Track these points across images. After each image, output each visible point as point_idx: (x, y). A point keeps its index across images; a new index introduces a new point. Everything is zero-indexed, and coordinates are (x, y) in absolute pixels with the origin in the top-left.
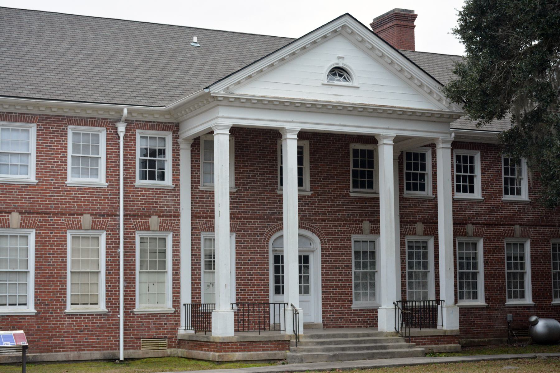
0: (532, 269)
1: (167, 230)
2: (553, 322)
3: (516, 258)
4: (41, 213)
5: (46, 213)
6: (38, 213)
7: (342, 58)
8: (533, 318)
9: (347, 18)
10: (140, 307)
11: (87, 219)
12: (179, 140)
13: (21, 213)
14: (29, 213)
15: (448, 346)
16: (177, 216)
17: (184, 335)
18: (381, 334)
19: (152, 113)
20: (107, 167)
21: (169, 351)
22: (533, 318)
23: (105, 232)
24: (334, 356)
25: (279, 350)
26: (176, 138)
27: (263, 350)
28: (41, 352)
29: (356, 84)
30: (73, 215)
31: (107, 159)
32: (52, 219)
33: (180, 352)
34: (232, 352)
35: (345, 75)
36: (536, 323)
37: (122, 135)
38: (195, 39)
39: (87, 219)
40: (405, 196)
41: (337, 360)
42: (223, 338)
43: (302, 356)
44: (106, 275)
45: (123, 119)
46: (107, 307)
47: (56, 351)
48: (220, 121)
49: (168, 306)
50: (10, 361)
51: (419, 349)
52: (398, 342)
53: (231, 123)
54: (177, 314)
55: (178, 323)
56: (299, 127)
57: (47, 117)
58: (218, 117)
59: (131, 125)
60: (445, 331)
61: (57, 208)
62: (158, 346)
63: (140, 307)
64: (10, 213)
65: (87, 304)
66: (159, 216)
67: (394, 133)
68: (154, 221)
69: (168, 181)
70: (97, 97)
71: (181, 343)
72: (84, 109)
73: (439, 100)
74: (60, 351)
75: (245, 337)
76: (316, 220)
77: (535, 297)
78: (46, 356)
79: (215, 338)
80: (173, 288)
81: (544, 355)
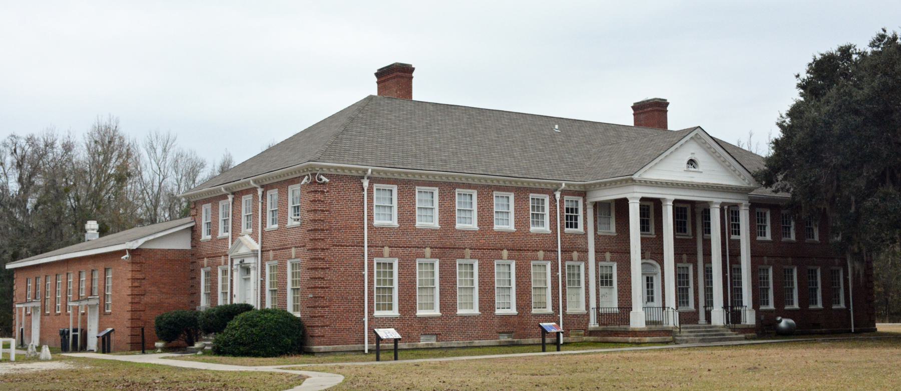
0: (774, 285)
1: (582, 260)
2: (791, 321)
3: (764, 278)
4: (519, 250)
5: (521, 250)
6: (516, 250)
7: (694, 154)
8: (779, 318)
9: (699, 129)
10: (569, 311)
11: (541, 254)
12: (586, 203)
13: (508, 250)
14: (512, 250)
15: (750, 334)
16: (586, 251)
17: (594, 328)
18: (715, 326)
19: (574, 186)
20: (550, 220)
21: (585, 338)
22: (779, 318)
23: (550, 262)
24: (703, 339)
25: (667, 336)
26: (585, 201)
27: (660, 336)
28: (521, 338)
29: (700, 170)
30: (534, 251)
31: (550, 215)
32: (524, 254)
33: (592, 338)
34: (644, 337)
35: (694, 164)
36: (780, 321)
37: (558, 200)
38: (557, 127)
39: (541, 254)
40: (705, 238)
41: (704, 342)
42: (640, 329)
43: (687, 339)
44: (552, 290)
45: (560, 189)
46: (553, 310)
47: (528, 338)
48: (635, 195)
49: (582, 309)
50: (506, 344)
51: (742, 336)
52: (727, 331)
53: (640, 196)
54: (588, 315)
55: (588, 320)
56: (673, 198)
57: (519, 188)
58: (634, 192)
59: (564, 193)
60: (748, 325)
61: (526, 247)
62: (578, 335)
63: (569, 311)
64: (502, 250)
65: (540, 308)
66: (578, 252)
67: (720, 201)
68: (575, 254)
69: (580, 229)
70: (543, 175)
71: (592, 333)
72: (539, 183)
73: (743, 180)
74: (529, 338)
75: (650, 328)
76: (658, 253)
77: (776, 303)
78: (523, 341)
79: (632, 328)
80: (586, 298)
81: (820, 339)
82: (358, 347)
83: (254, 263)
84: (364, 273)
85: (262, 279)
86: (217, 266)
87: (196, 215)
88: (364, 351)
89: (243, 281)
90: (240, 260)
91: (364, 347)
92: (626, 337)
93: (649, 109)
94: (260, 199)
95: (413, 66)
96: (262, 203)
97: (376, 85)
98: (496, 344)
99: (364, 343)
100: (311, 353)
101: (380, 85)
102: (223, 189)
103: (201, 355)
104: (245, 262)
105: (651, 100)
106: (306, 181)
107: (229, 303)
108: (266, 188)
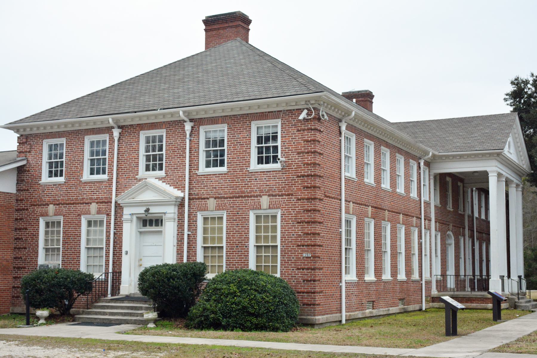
82: (334, 317)
83: (175, 213)
84: (340, 230)
85: (190, 233)
86: (79, 215)
87: (29, 152)
88: (340, 321)
89: (138, 233)
90: (145, 208)
91: (341, 316)
92: (483, 303)
93: (361, 99)
94: (188, 136)
95: (250, 18)
96: (190, 140)
97: (204, 32)
98: (398, 311)
99: (340, 311)
100: (312, 325)
101: (209, 33)
102: (110, 120)
103: (154, 328)
104: (150, 211)
105: (363, 91)
106: (306, 116)
107: (185, 261)
108: (198, 122)
